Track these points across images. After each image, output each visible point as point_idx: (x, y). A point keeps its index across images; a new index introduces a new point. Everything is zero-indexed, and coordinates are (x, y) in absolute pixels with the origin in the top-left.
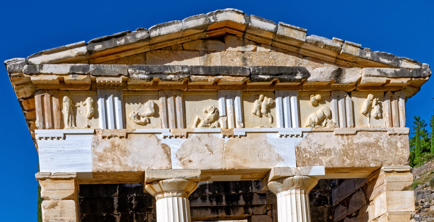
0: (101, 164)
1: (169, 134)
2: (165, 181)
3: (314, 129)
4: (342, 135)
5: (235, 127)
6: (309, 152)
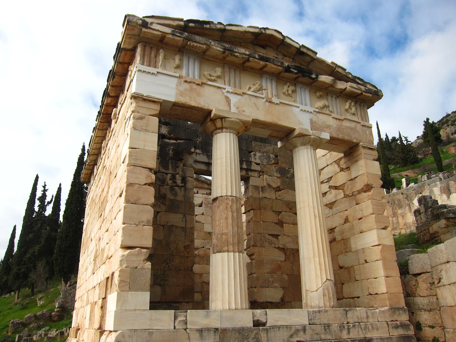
0: (181, 98)
1: (231, 91)
2: (228, 119)
4: (336, 119)
6: (318, 124)
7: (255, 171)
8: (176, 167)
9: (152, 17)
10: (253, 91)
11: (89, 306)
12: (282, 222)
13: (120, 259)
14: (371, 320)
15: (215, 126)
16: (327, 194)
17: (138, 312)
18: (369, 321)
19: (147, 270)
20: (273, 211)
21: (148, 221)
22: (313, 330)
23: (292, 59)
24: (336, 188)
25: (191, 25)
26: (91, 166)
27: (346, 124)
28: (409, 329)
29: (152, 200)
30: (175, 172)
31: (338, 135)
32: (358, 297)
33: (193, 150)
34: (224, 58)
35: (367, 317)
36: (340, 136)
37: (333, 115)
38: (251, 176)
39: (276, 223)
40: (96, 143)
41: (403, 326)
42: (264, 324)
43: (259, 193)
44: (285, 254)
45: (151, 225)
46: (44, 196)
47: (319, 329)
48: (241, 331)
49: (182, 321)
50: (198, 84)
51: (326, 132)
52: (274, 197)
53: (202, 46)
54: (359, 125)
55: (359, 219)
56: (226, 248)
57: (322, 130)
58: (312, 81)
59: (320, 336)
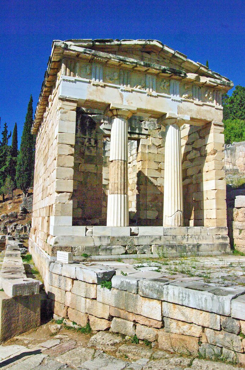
0: (90, 97)
1: (124, 89)
4: (197, 105)
7: (144, 134)
8: (91, 134)
10: (139, 89)
11: (41, 218)
12: (161, 169)
13: (55, 199)
14: (202, 234)
15: (113, 113)
16: (190, 153)
17: (66, 227)
18: (202, 234)
19: (71, 205)
20: (155, 162)
21: (71, 177)
22: (166, 239)
23: (170, 60)
24: (196, 149)
25: (97, 43)
26: (38, 125)
27: (205, 108)
28: (227, 240)
29: (72, 165)
30: (90, 137)
31: (197, 116)
32: (201, 219)
33: (102, 121)
34: (120, 65)
35: (201, 232)
36: (198, 117)
38: (141, 138)
40: (40, 112)
41: (223, 238)
42: (137, 235)
45: (72, 178)
47: (169, 238)
48: (123, 238)
49: (90, 232)
50: (102, 86)
51: (188, 115)
52: (156, 153)
54: (213, 108)
55: (207, 172)
56: (116, 192)
57: (186, 113)
58: (181, 78)
59: (169, 242)
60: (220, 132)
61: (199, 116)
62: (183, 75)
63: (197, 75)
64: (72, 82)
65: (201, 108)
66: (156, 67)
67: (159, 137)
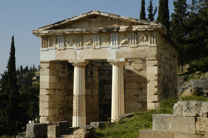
0: (57, 58)
1: (77, 49)
3: (123, 46)
4: (132, 47)
5: (97, 45)
9: (41, 28)
27: (140, 48)
29: (48, 100)
31: (132, 56)
37: (131, 46)
38: (126, 65)
39: (138, 89)
43: (129, 74)
44: (142, 104)
46: (151, 7)
50: (63, 50)
53: (60, 34)
54: (147, 47)
60: (153, 65)
61: (134, 56)
62: (116, 30)
63: (129, 26)
64: (46, 50)
65: (136, 49)
66: (95, 29)
67: (140, 62)
